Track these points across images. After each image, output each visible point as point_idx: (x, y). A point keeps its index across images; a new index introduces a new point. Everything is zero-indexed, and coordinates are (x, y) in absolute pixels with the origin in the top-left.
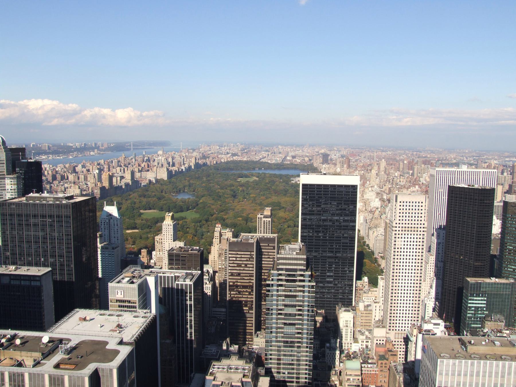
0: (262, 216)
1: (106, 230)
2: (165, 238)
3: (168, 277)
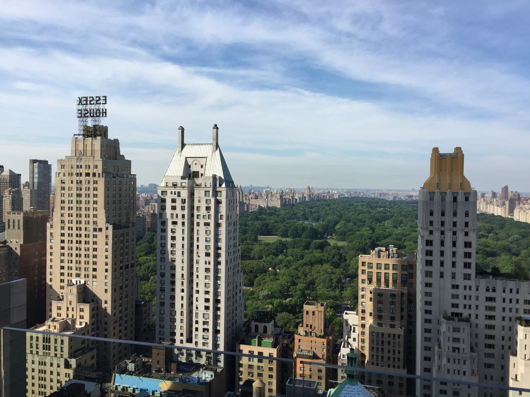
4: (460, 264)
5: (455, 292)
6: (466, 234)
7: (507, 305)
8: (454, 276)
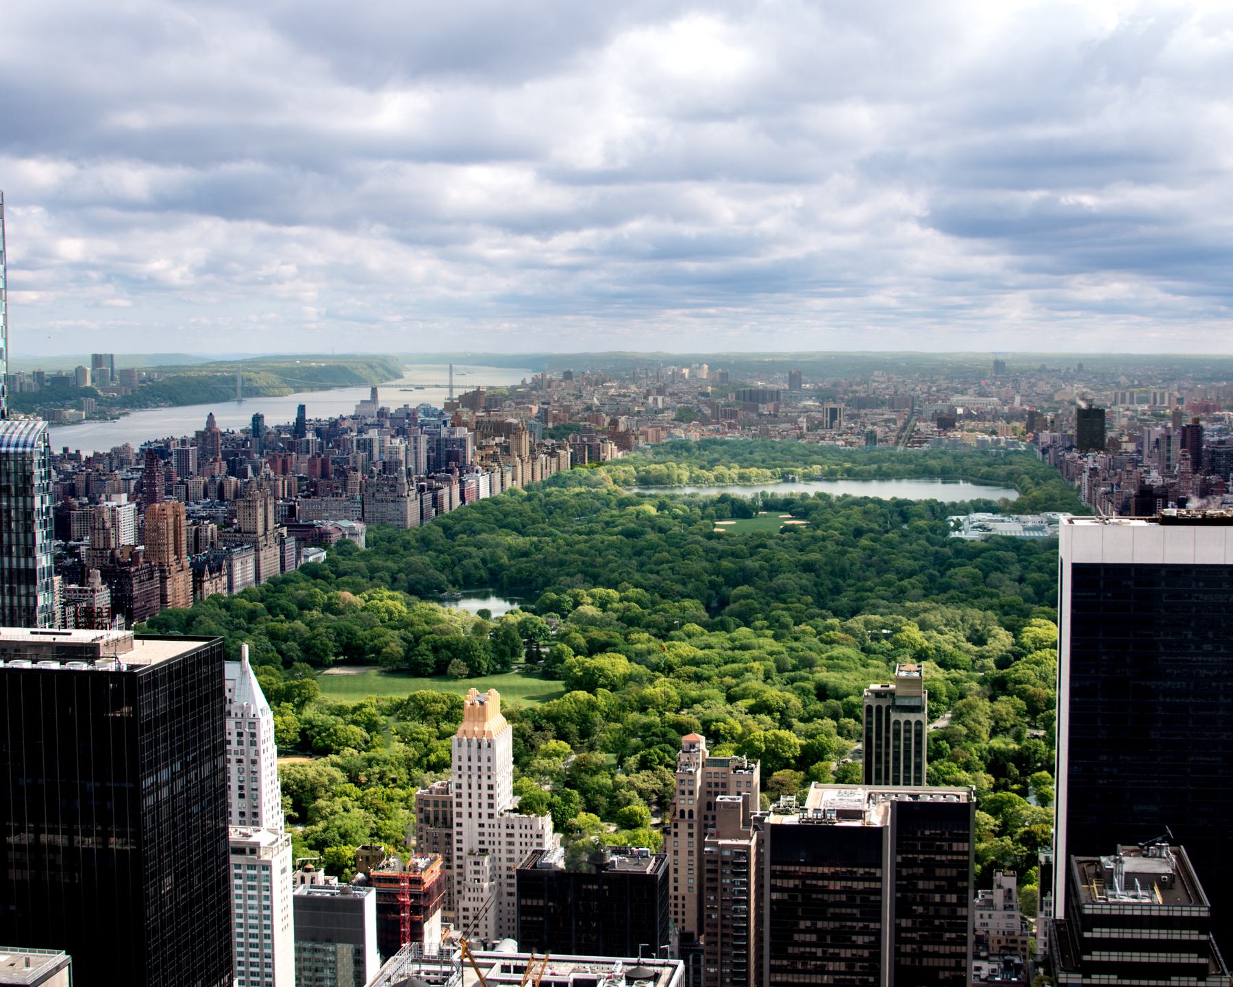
0: (884, 703)
2: (465, 800)
4: (485, 805)
5: (481, 830)
6: (489, 777)
7: (524, 840)
8: (480, 815)
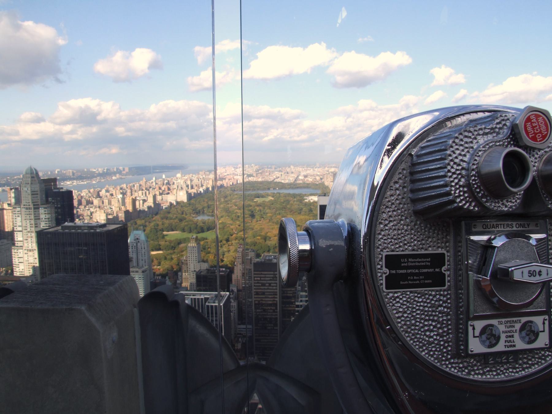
1: (134, 253)
3: (198, 299)
